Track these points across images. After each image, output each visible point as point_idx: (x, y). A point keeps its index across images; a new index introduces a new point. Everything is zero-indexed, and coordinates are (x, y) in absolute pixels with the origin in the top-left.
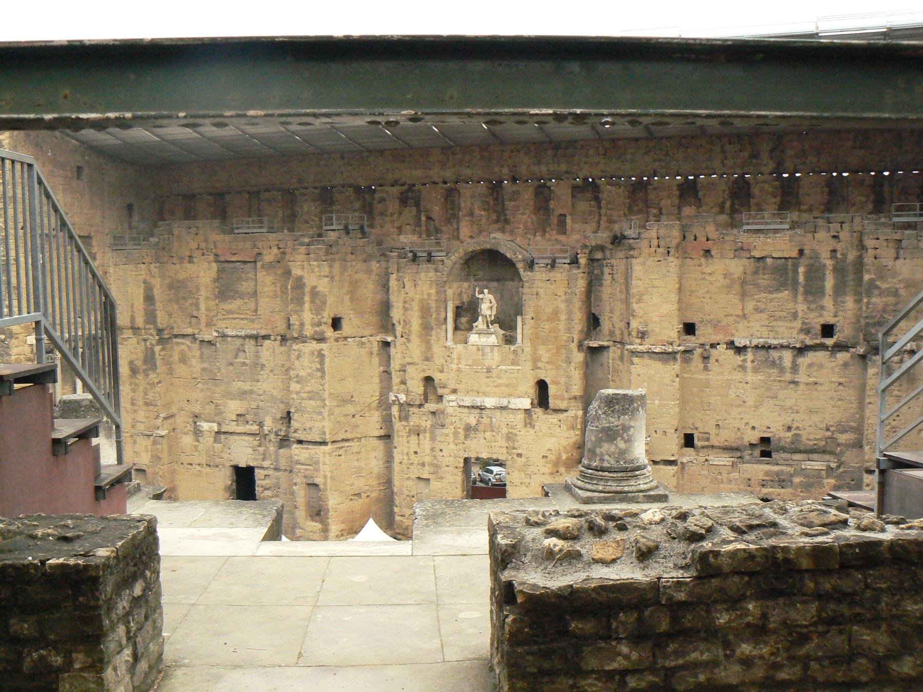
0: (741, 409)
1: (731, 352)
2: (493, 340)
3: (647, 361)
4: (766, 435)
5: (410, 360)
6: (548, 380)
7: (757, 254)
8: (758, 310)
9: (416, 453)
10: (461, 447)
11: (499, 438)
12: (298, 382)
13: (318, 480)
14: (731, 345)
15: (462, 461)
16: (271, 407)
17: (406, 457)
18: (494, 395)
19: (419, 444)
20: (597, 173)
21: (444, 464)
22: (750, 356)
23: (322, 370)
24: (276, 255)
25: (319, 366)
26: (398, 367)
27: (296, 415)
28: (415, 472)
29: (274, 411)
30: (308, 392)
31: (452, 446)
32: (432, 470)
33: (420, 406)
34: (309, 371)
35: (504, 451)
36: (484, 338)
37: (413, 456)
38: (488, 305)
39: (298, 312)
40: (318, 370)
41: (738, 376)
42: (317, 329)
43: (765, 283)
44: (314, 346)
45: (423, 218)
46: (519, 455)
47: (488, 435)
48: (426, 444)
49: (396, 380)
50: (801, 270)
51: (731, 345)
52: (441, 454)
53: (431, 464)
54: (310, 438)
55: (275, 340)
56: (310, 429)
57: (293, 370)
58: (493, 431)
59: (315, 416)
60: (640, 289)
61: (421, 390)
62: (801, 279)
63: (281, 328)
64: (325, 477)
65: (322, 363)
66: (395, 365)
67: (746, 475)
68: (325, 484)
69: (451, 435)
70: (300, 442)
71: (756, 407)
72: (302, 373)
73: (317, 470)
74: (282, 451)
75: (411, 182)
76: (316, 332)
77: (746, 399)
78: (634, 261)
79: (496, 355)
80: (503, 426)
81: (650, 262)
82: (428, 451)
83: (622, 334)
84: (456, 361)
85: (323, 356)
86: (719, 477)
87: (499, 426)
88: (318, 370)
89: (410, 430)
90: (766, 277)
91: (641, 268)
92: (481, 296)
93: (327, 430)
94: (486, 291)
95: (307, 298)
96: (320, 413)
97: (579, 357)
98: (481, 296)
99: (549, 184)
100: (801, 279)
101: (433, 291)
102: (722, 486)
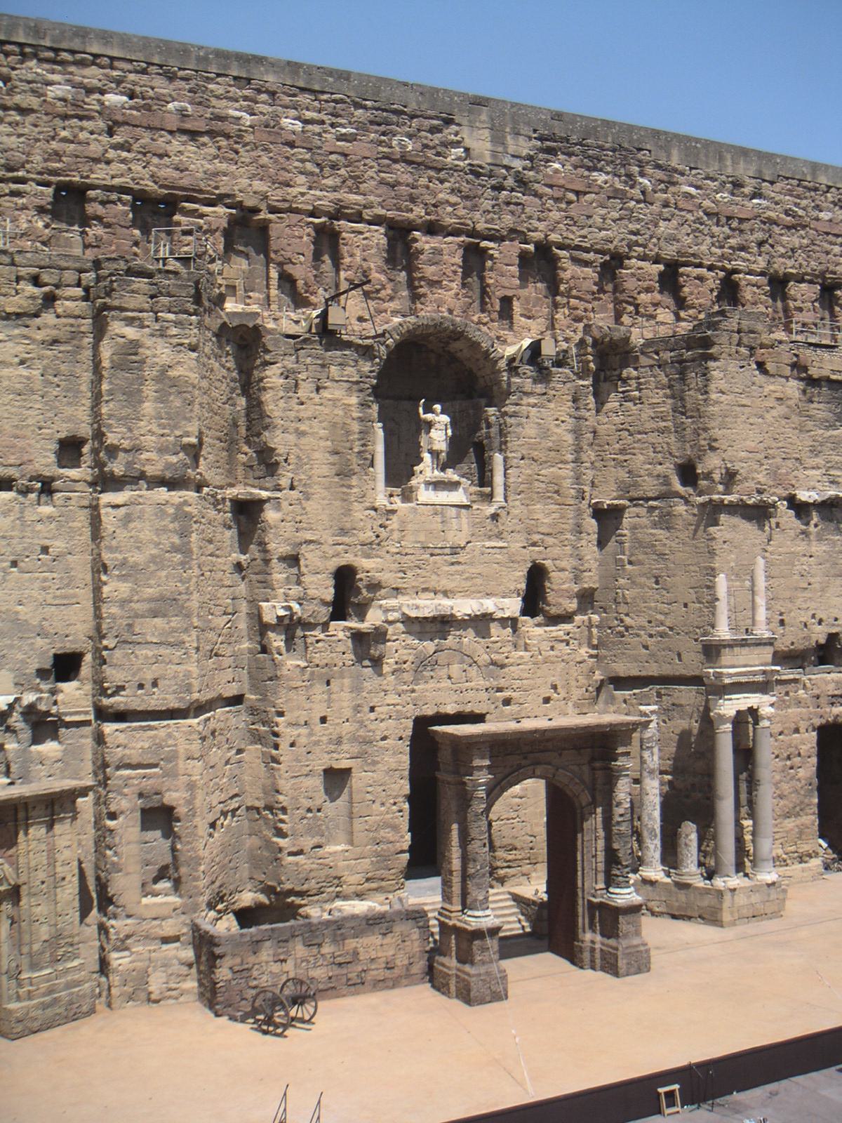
0: (807, 594)
1: (792, 512)
2: (458, 497)
3: (736, 520)
4: (834, 630)
5: (309, 536)
6: (548, 563)
7: (814, 372)
8: (815, 452)
9: (323, 720)
10: (406, 698)
12: (123, 578)
13: (170, 798)
14: (793, 502)
15: (410, 724)
16: (12, 647)
17: (304, 731)
18: (466, 593)
19: (329, 701)
20: (554, 237)
21: (379, 735)
23: (184, 549)
24: (33, 298)
25: (176, 540)
26: (285, 549)
27: (118, 653)
28: (321, 761)
29: (20, 656)
30: (150, 600)
31: (392, 699)
32: (355, 749)
33: (325, 627)
34: (154, 551)
35: (484, 695)
37: (319, 727)
38: (439, 429)
39: (129, 422)
40: (175, 549)
41: (801, 547)
42: (174, 459)
43: (821, 415)
44: (162, 493)
45: (274, 274)
46: (507, 702)
47: (455, 669)
48: (344, 698)
51: (793, 502)
52: (372, 716)
53: (354, 739)
54: (155, 701)
55: (25, 492)
56: (155, 684)
57: (111, 549)
58: (462, 662)
59: (163, 651)
60: (723, 407)
61: (329, 594)
63: (45, 461)
64: (191, 787)
65: (184, 534)
66: (278, 547)
67: (816, 692)
68: (190, 802)
70: (121, 716)
71: (823, 590)
72: (136, 558)
73: (172, 774)
74: (34, 748)
75: (250, 203)
76: (168, 466)
77: (812, 580)
78: (711, 364)
79: (464, 521)
81: (733, 366)
82: (348, 713)
83: (666, 481)
84: (396, 535)
85: (188, 516)
86: (787, 698)
87: (474, 651)
88: (175, 549)
89: (312, 673)
90: (821, 406)
91: (721, 375)
92: (429, 416)
93: (196, 684)
94: (438, 407)
95: (149, 390)
96: (179, 644)
97: (591, 524)
98: (429, 416)
99: (484, 244)
101: (354, 400)
102: (790, 710)
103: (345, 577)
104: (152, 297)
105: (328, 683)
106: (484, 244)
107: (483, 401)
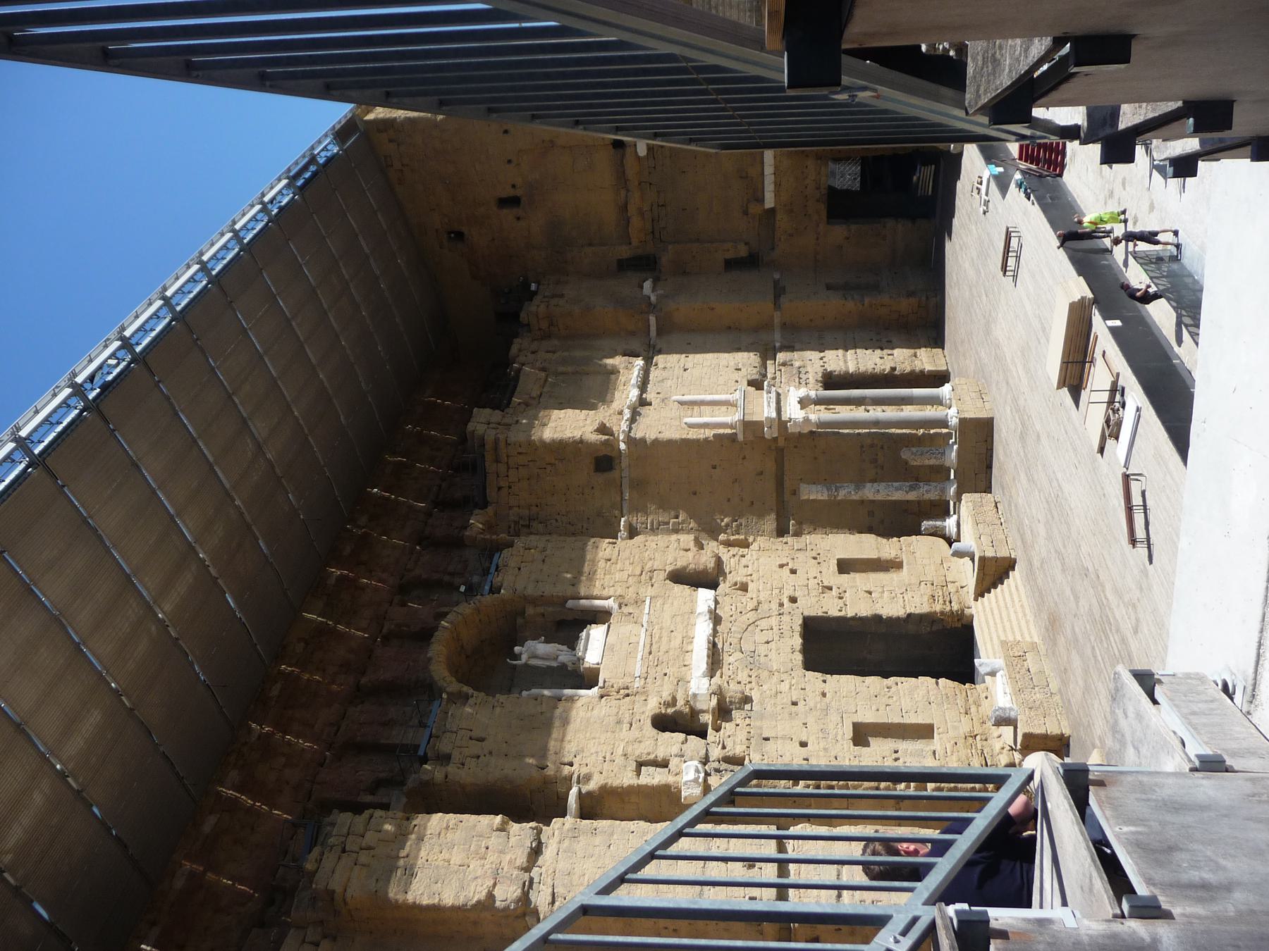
6: (669, 568)
9: (803, 744)
11: (763, 624)
22: (649, 396)
35: (786, 618)
36: (595, 646)
38: (537, 651)
49: (653, 777)
50: (561, 369)
62: (570, 369)
66: (627, 778)
69: (765, 687)
80: (744, 618)
98: (524, 658)
99: (385, 631)
100: (570, 369)
103: (663, 723)
104: (344, 851)
105: (767, 739)
106: (385, 631)
107: (520, 621)
